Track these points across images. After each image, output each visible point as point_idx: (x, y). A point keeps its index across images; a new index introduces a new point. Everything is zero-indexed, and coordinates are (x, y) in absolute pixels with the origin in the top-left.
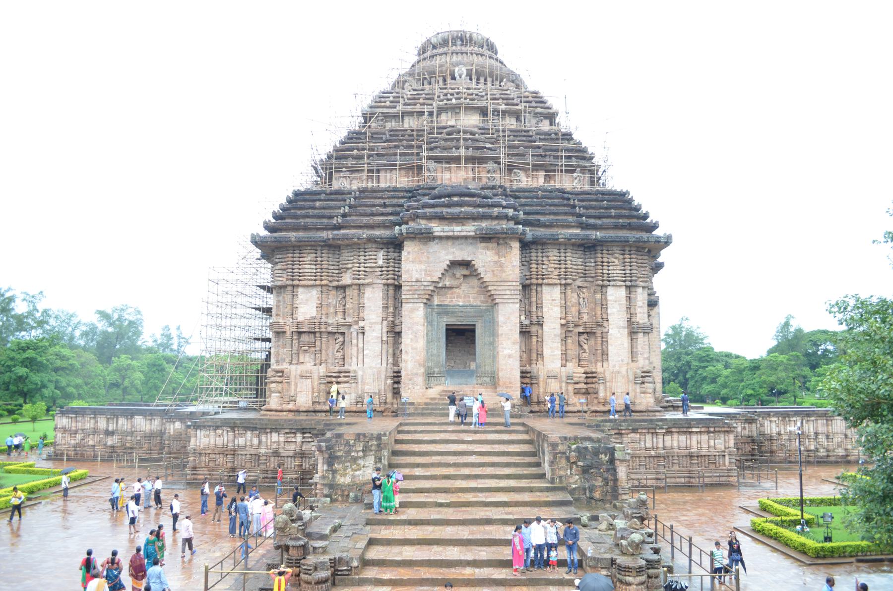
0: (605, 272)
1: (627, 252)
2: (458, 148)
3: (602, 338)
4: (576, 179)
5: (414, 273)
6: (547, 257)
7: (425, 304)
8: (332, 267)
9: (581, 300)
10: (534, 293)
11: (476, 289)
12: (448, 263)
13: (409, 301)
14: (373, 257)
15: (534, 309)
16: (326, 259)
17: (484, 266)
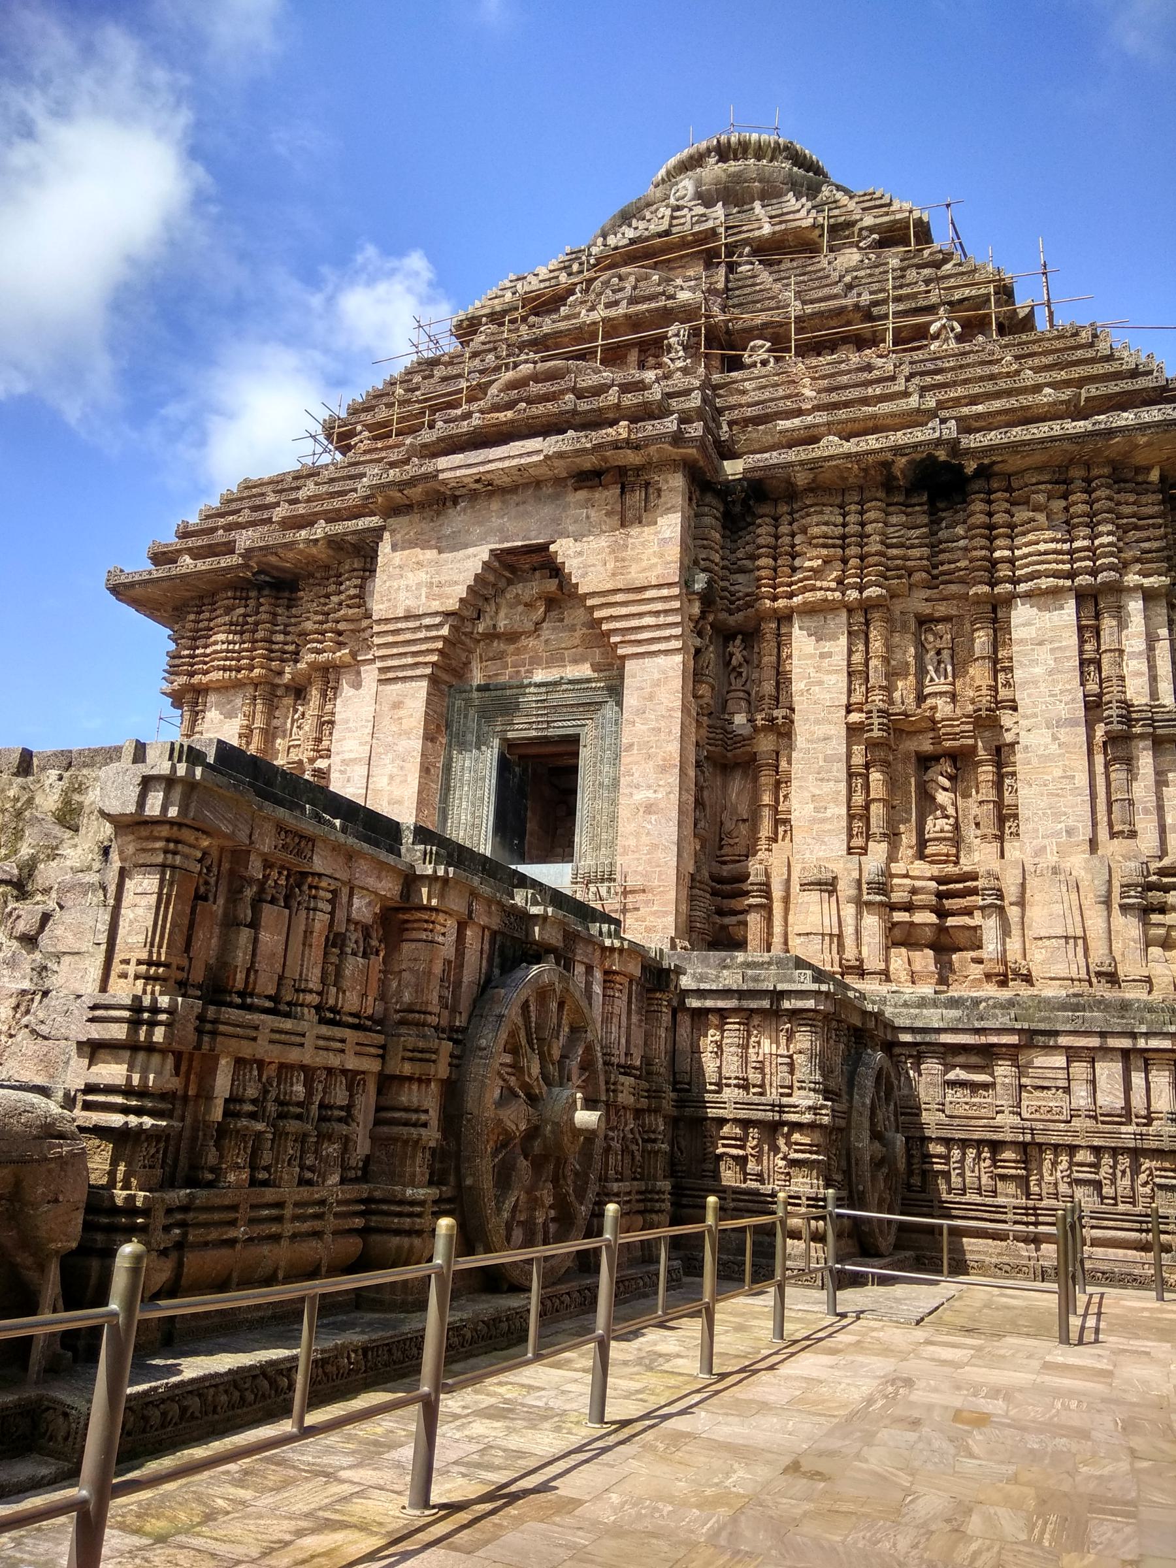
0: (997, 554)
1: (1079, 484)
2: (592, 308)
3: (999, 765)
4: (936, 337)
5: (402, 595)
6: (804, 531)
7: (433, 680)
8: (280, 638)
9: (932, 653)
10: (768, 646)
11: (578, 634)
12: (486, 557)
13: (390, 675)
14: (352, 592)
15: (768, 687)
16: (264, 616)
17: (580, 554)
